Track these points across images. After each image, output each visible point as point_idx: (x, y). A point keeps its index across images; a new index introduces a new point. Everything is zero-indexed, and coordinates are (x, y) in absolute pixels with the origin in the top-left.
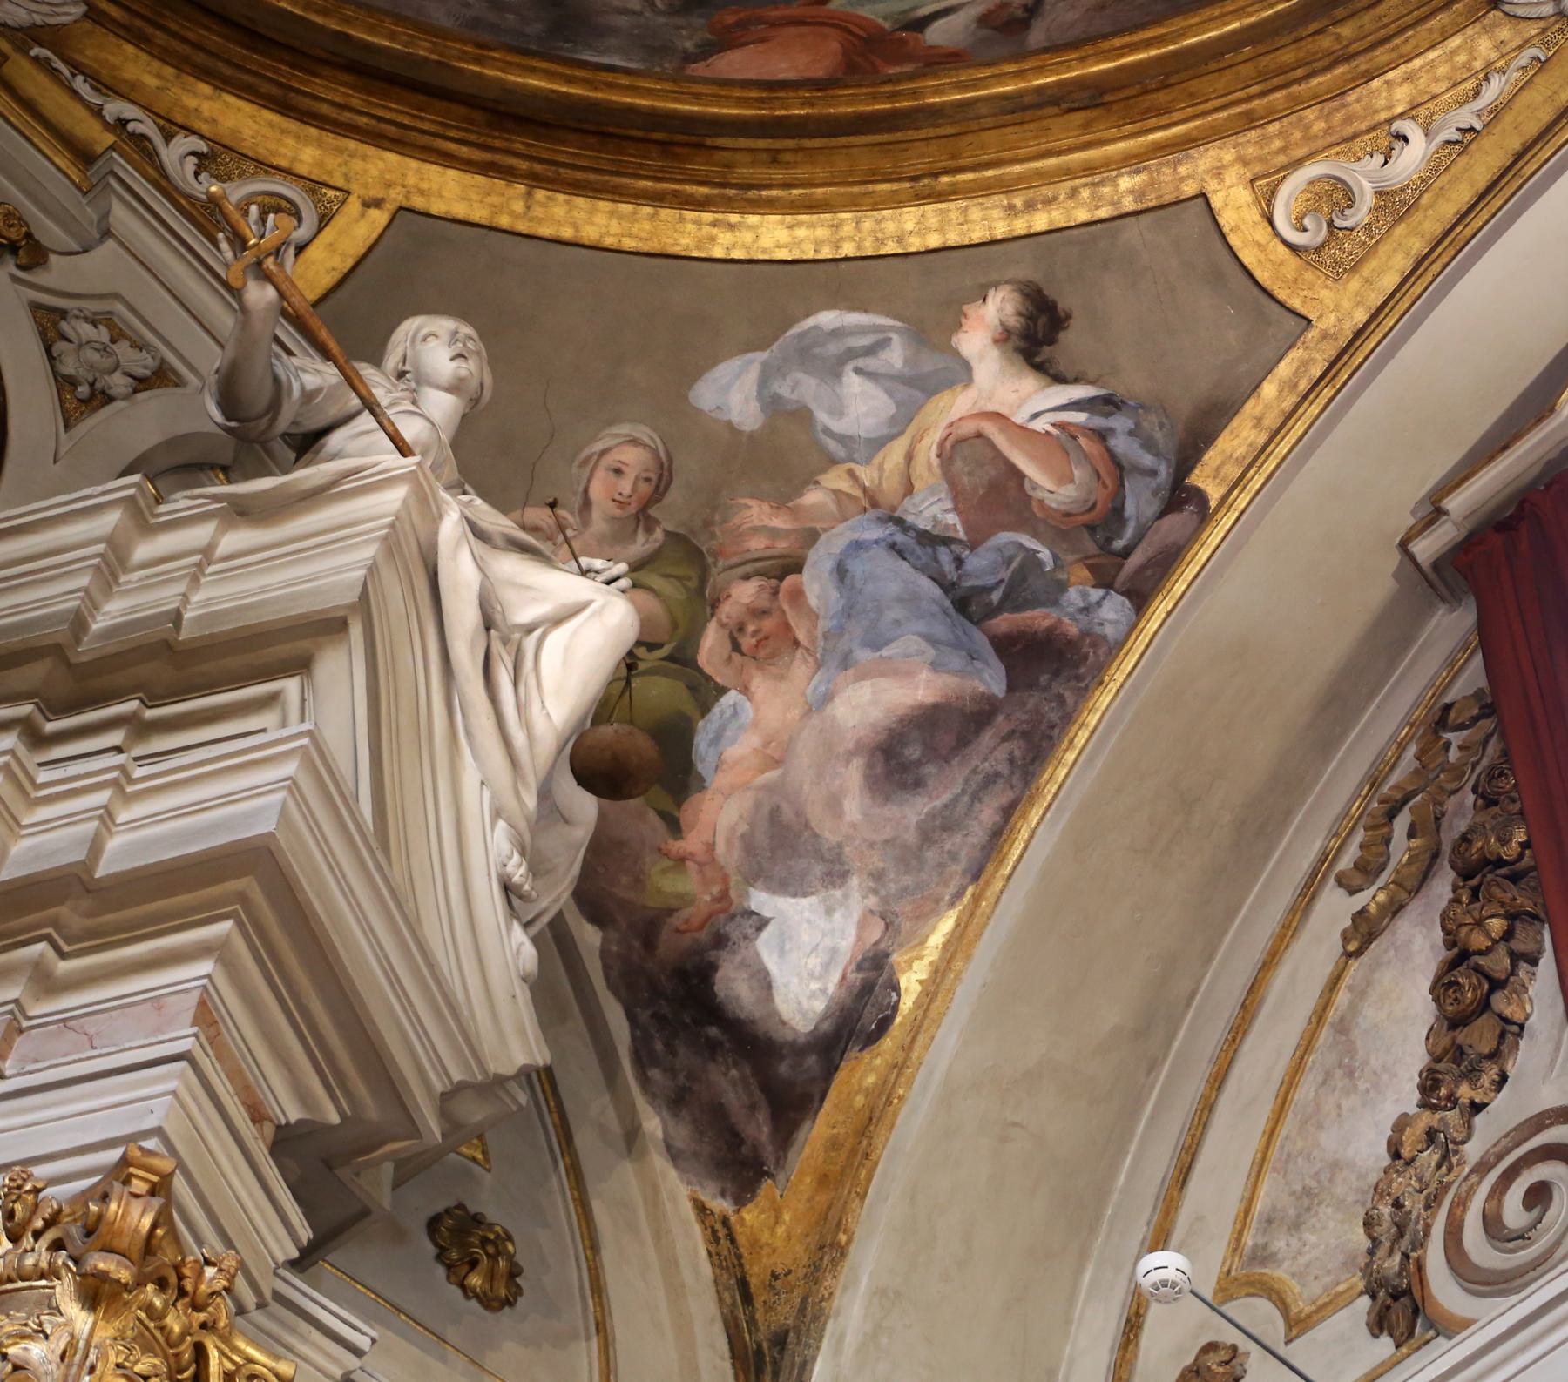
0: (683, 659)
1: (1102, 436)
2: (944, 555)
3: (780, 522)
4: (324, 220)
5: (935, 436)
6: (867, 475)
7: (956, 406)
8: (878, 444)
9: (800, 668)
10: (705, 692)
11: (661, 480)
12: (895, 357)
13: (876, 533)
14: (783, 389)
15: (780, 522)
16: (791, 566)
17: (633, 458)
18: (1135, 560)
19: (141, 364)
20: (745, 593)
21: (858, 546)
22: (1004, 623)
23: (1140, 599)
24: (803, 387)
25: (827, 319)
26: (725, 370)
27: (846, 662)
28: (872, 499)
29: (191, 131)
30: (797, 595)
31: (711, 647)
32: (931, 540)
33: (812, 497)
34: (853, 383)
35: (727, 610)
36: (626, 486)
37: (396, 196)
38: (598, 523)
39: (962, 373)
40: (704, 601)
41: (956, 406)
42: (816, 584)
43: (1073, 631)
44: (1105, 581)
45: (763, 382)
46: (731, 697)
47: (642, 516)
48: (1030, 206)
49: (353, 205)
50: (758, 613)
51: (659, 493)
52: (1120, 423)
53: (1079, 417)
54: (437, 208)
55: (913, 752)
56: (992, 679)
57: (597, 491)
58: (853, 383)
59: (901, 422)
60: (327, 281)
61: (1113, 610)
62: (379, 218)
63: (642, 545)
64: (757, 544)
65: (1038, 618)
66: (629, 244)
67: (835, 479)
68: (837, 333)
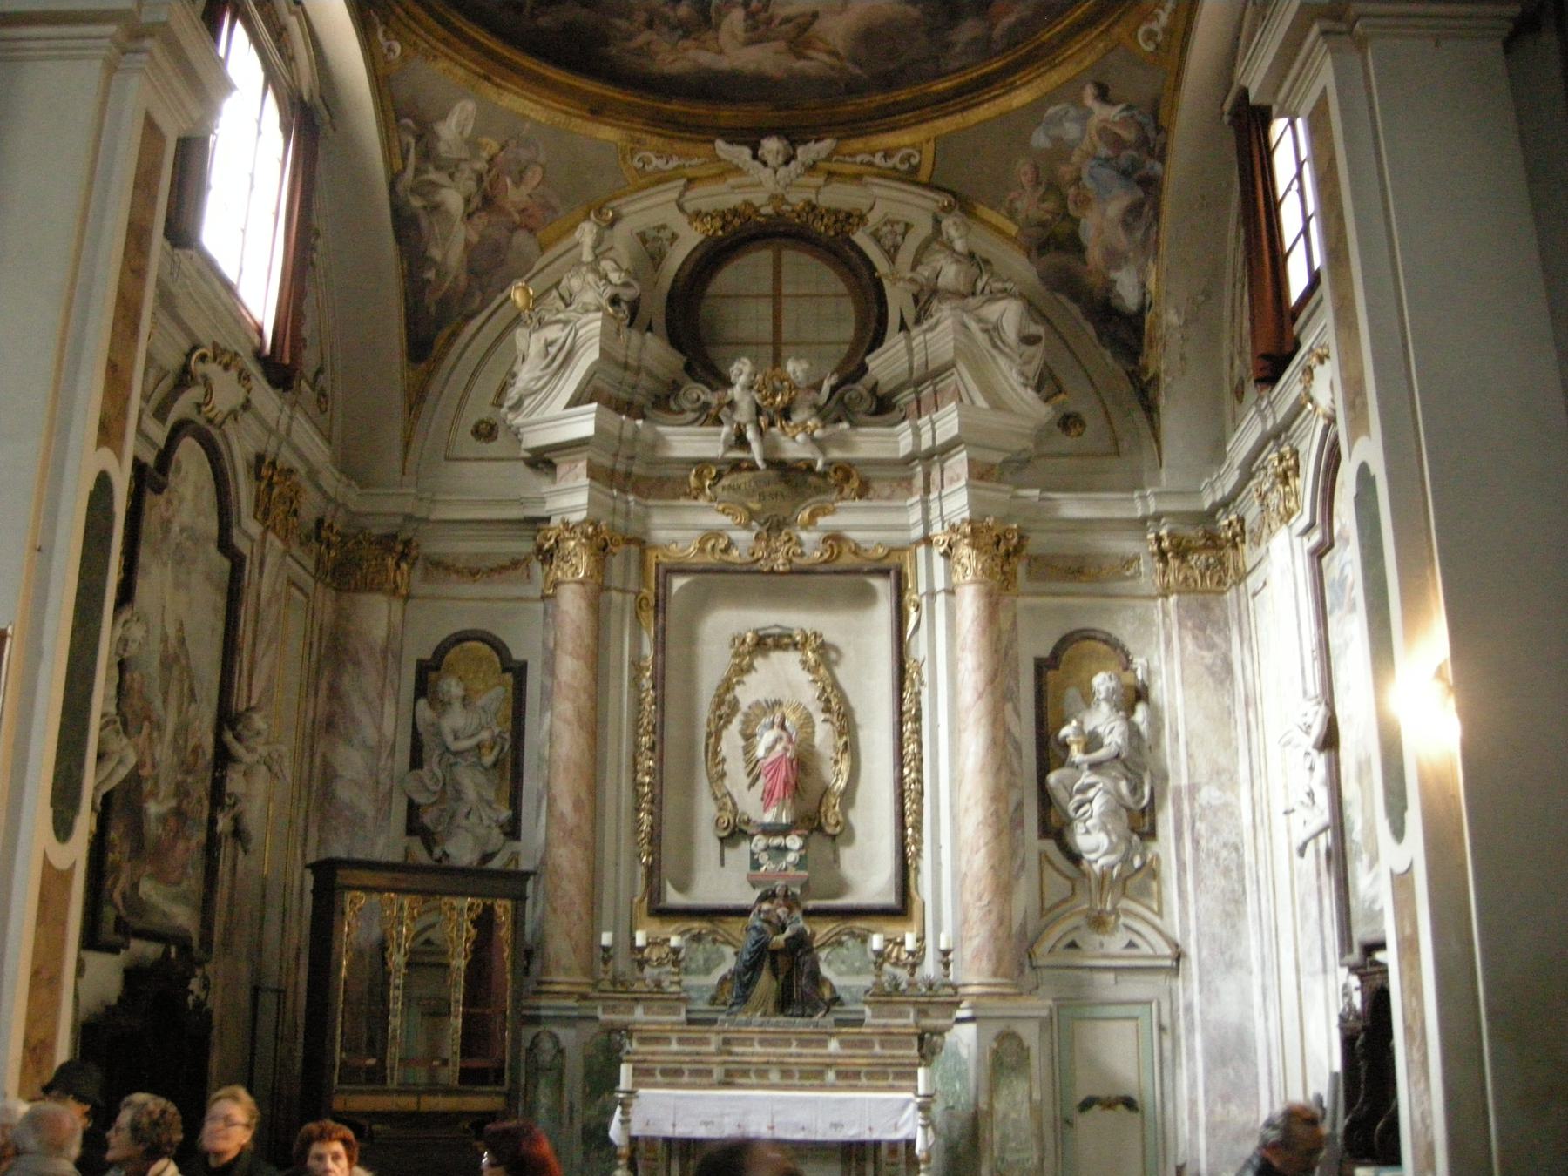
0: (1066, 216)
1: (1132, 117)
2: (1113, 163)
3: (1071, 168)
4: (920, 152)
5: (1093, 132)
6: (1084, 148)
7: (1094, 122)
8: (1081, 139)
9: (1094, 206)
10: (1076, 221)
11: (1036, 168)
12: (1073, 112)
13: (1093, 163)
14: (1051, 133)
15: (1071, 168)
16: (1079, 179)
17: (1026, 168)
18: (1157, 149)
19: (900, 229)
20: (1072, 191)
21: (1092, 167)
22: (1135, 176)
23: (1162, 158)
24: (1055, 132)
25: (1051, 110)
26: (1035, 134)
27: (1105, 200)
28: (1088, 153)
29: (878, 151)
30: (1085, 187)
31: (1071, 207)
32: (1107, 159)
33: (1075, 159)
34: (1067, 125)
35: (1070, 197)
36: (1029, 176)
37: (932, 135)
38: (1028, 189)
39: (1090, 112)
40: (1063, 199)
41: (1094, 122)
42: (1087, 182)
43: (1151, 174)
44: (1151, 154)
45: (1047, 135)
46: (1083, 221)
47: (1038, 183)
48: (1081, 61)
49: (925, 146)
50: (1078, 194)
51: (1038, 176)
52: (1135, 112)
53: (1125, 114)
54: (944, 131)
55: (1130, 219)
56: (1139, 193)
57: (1024, 182)
58: (1067, 125)
59: (1084, 131)
60: (930, 167)
61: (1158, 167)
62: (932, 144)
63: (1041, 190)
64: (1068, 177)
65: (1142, 172)
66: (993, 115)
67: (1077, 152)
68: (1056, 113)
